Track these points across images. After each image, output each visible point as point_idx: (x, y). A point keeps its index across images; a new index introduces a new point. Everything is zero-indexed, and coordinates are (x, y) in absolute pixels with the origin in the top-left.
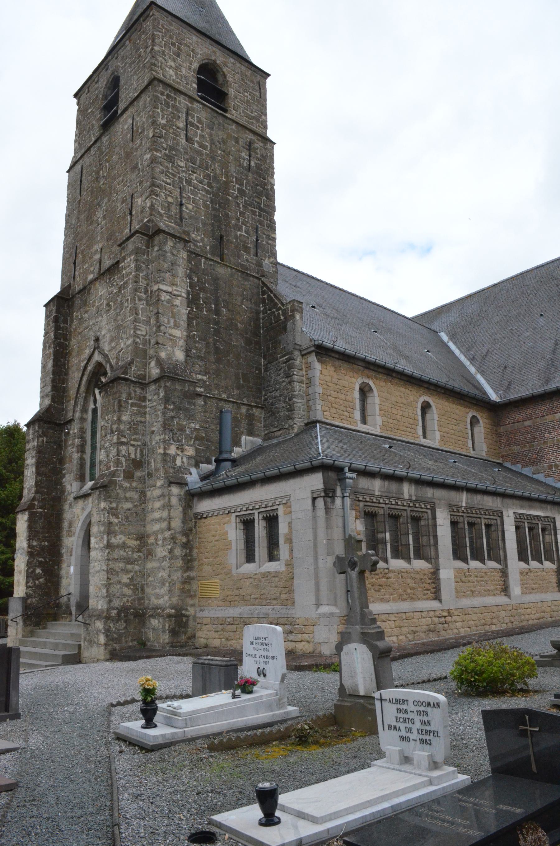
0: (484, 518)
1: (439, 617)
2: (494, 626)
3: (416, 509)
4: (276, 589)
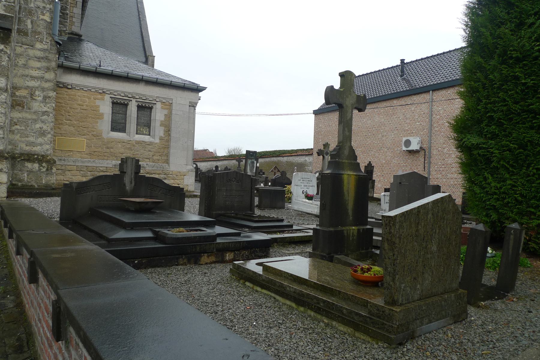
4: (150, 152)
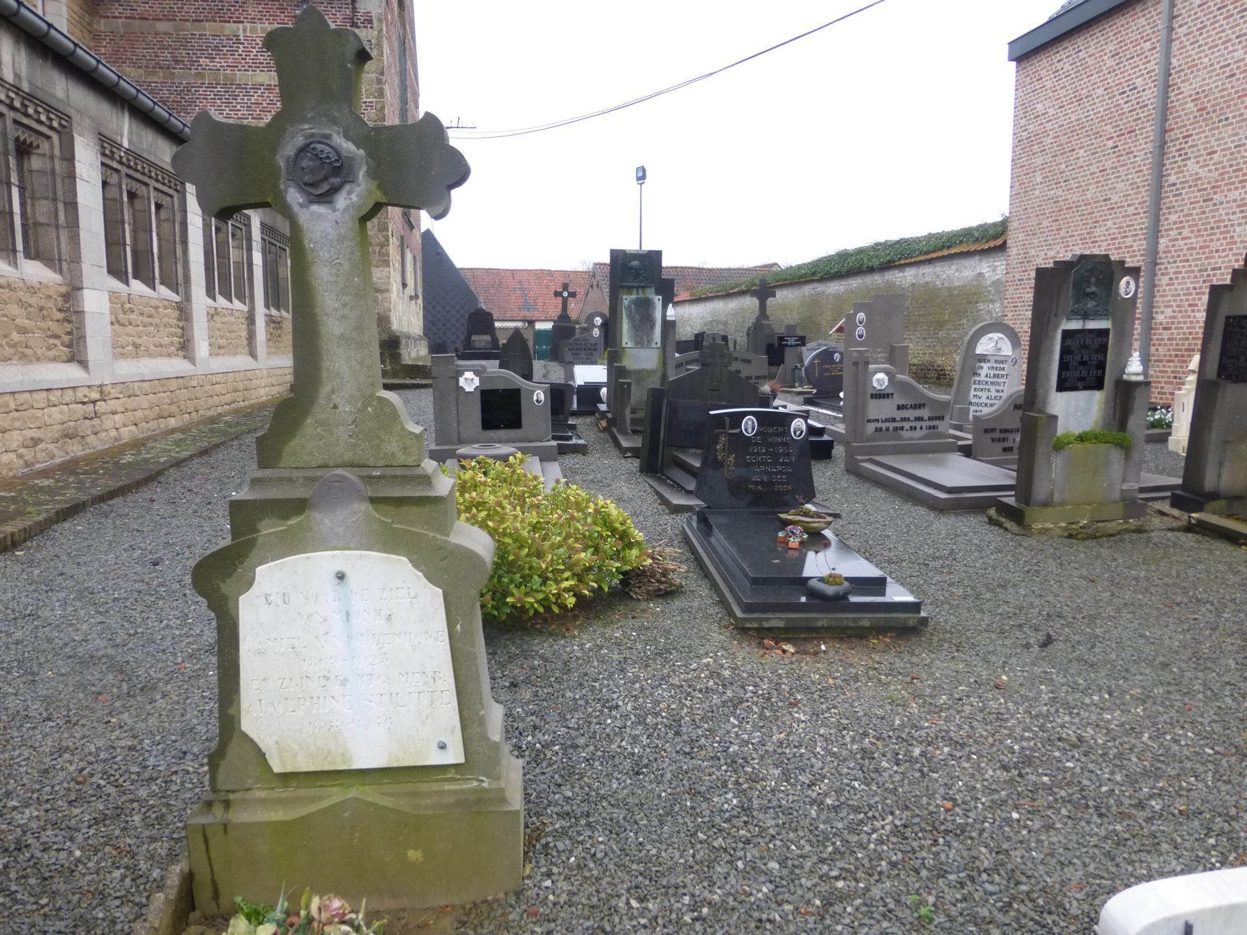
0: (155, 189)
1: (84, 403)
2: (172, 420)
3: (25, 121)
